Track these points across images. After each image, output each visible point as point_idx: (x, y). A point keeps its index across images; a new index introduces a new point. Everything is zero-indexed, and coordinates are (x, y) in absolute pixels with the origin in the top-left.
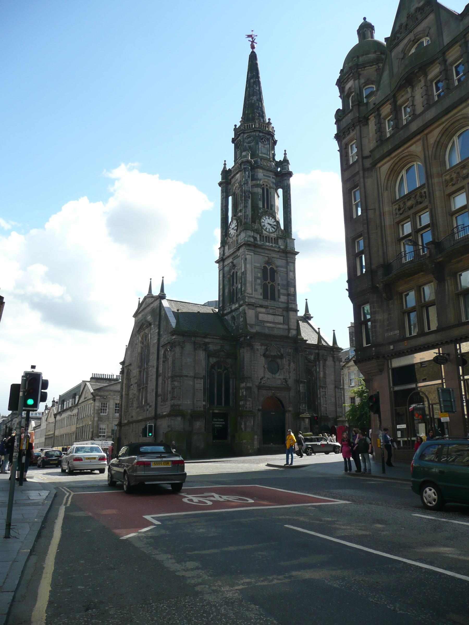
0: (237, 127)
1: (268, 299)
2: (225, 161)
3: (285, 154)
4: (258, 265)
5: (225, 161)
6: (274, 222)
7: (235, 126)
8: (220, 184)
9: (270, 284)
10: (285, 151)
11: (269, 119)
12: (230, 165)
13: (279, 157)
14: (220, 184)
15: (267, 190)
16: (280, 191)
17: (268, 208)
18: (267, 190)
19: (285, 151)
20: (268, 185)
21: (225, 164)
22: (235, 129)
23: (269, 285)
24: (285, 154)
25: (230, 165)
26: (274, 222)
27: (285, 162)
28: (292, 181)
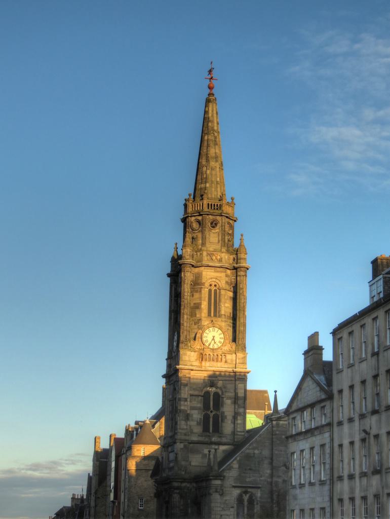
1: (209, 431)
6: (221, 334)
8: (169, 275)
9: (213, 413)
10: (242, 235)
14: (169, 275)
17: (215, 315)
18: (215, 291)
20: (218, 286)
23: (211, 415)
26: (221, 334)
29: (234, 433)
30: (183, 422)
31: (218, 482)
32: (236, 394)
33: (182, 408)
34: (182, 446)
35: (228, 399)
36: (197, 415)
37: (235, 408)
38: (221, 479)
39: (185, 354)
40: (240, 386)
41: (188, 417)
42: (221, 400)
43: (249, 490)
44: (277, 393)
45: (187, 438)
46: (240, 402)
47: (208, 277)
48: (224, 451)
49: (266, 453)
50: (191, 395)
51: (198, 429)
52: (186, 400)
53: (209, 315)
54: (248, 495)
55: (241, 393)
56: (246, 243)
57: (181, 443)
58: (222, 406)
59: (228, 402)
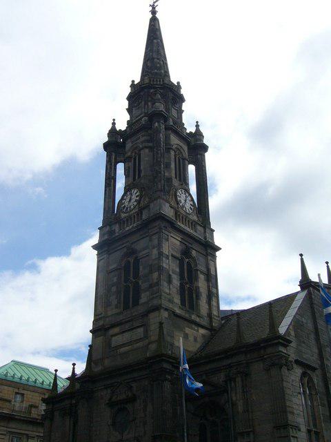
0: (136, 83)
2: (114, 120)
3: (197, 126)
4: (175, 254)
5: (114, 120)
7: (133, 81)
11: (178, 83)
12: (122, 126)
13: (190, 129)
15: (179, 160)
16: (191, 169)
17: (180, 180)
19: (197, 122)
21: (114, 124)
22: (133, 85)
24: (197, 126)
25: (122, 126)
27: (198, 134)
28: (209, 157)
29: (210, 315)
30: (166, 284)
31: (282, 349)
32: (208, 270)
33: (164, 265)
34: (165, 314)
35: (201, 272)
36: (176, 282)
37: (208, 286)
38: (286, 346)
39: (165, 206)
40: (211, 263)
41: (170, 282)
42: (194, 272)
43: (309, 372)
44: (303, 257)
45: (171, 306)
46: (213, 281)
47: (175, 143)
48: (203, 336)
49: (310, 325)
50: (172, 256)
51: (177, 300)
52: (167, 257)
53: (176, 178)
54: (306, 379)
55: (213, 272)
56: (201, 129)
57: (166, 309)
58: (197, 279)
59: (202, 277)
